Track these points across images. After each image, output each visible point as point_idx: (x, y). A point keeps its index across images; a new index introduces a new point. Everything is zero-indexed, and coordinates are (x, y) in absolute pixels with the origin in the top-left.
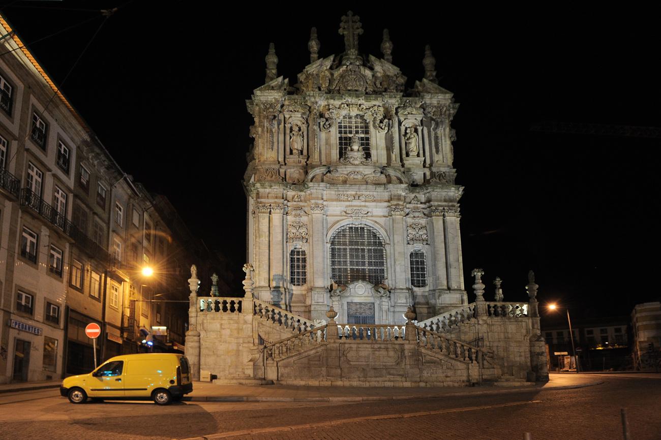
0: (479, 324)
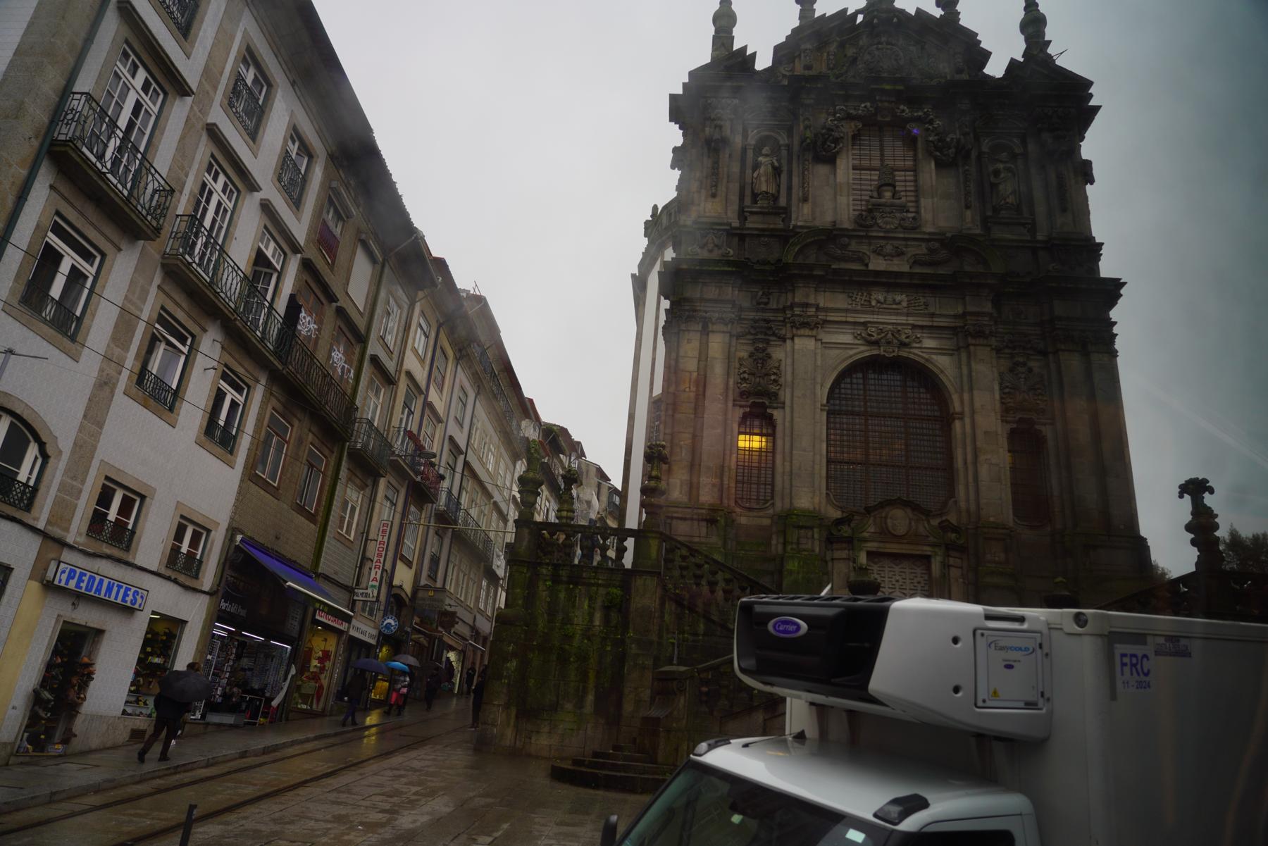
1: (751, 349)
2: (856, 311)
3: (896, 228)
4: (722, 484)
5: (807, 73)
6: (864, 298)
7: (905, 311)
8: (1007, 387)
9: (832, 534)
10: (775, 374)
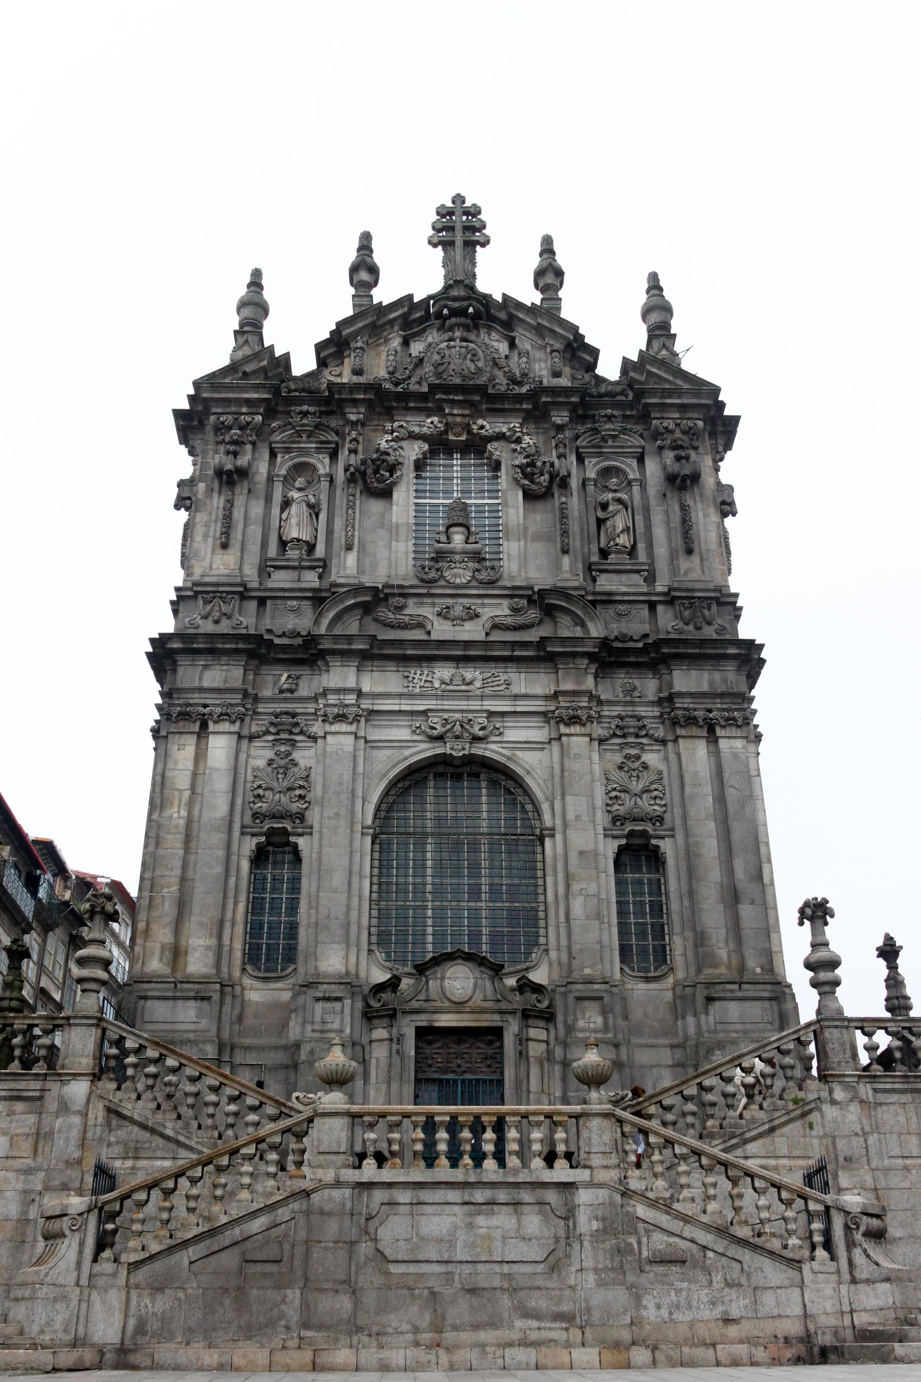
0: (833, 1102)
1: (270, 754)
2: (411, 696)
3: (469, 581)
4: (220, 945)
5: (356, 379)
6: (424, 678)
7: (478, 692)
8: (614, 789)
9: (369, 1006)
10: (301, 787)
